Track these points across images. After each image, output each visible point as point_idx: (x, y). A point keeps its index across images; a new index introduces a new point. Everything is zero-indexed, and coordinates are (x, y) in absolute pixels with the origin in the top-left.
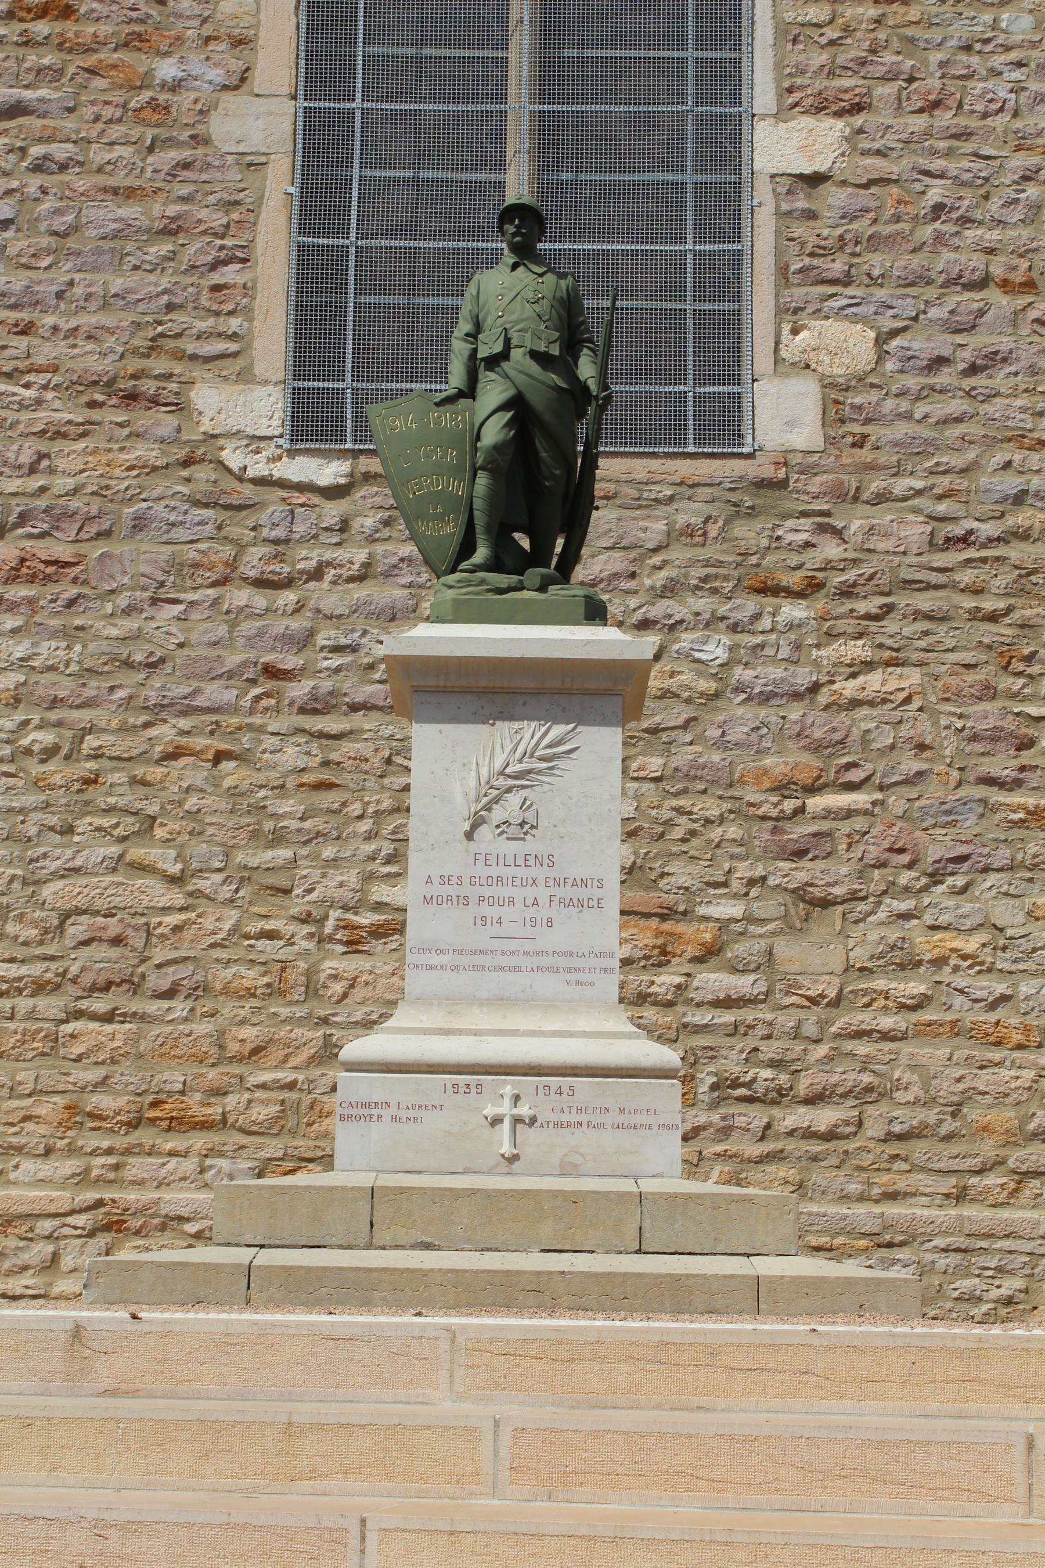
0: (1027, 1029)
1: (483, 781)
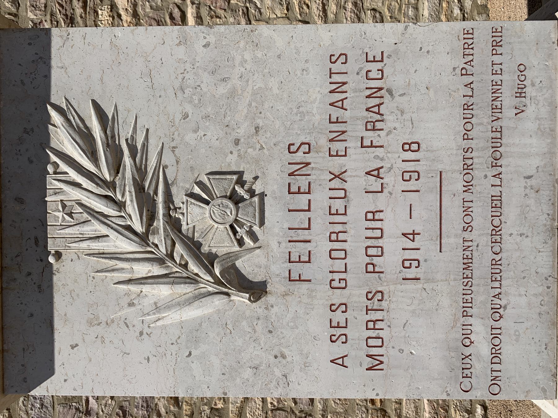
1: (157, 270)
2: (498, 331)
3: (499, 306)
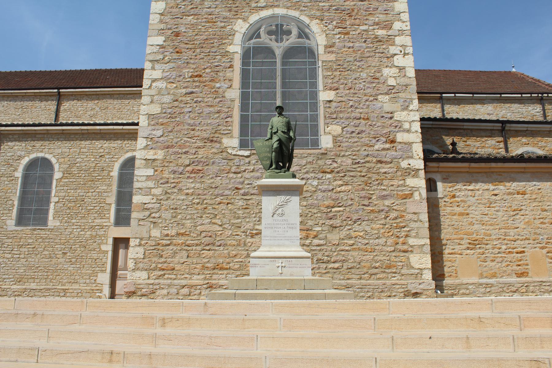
0: (371, 249)
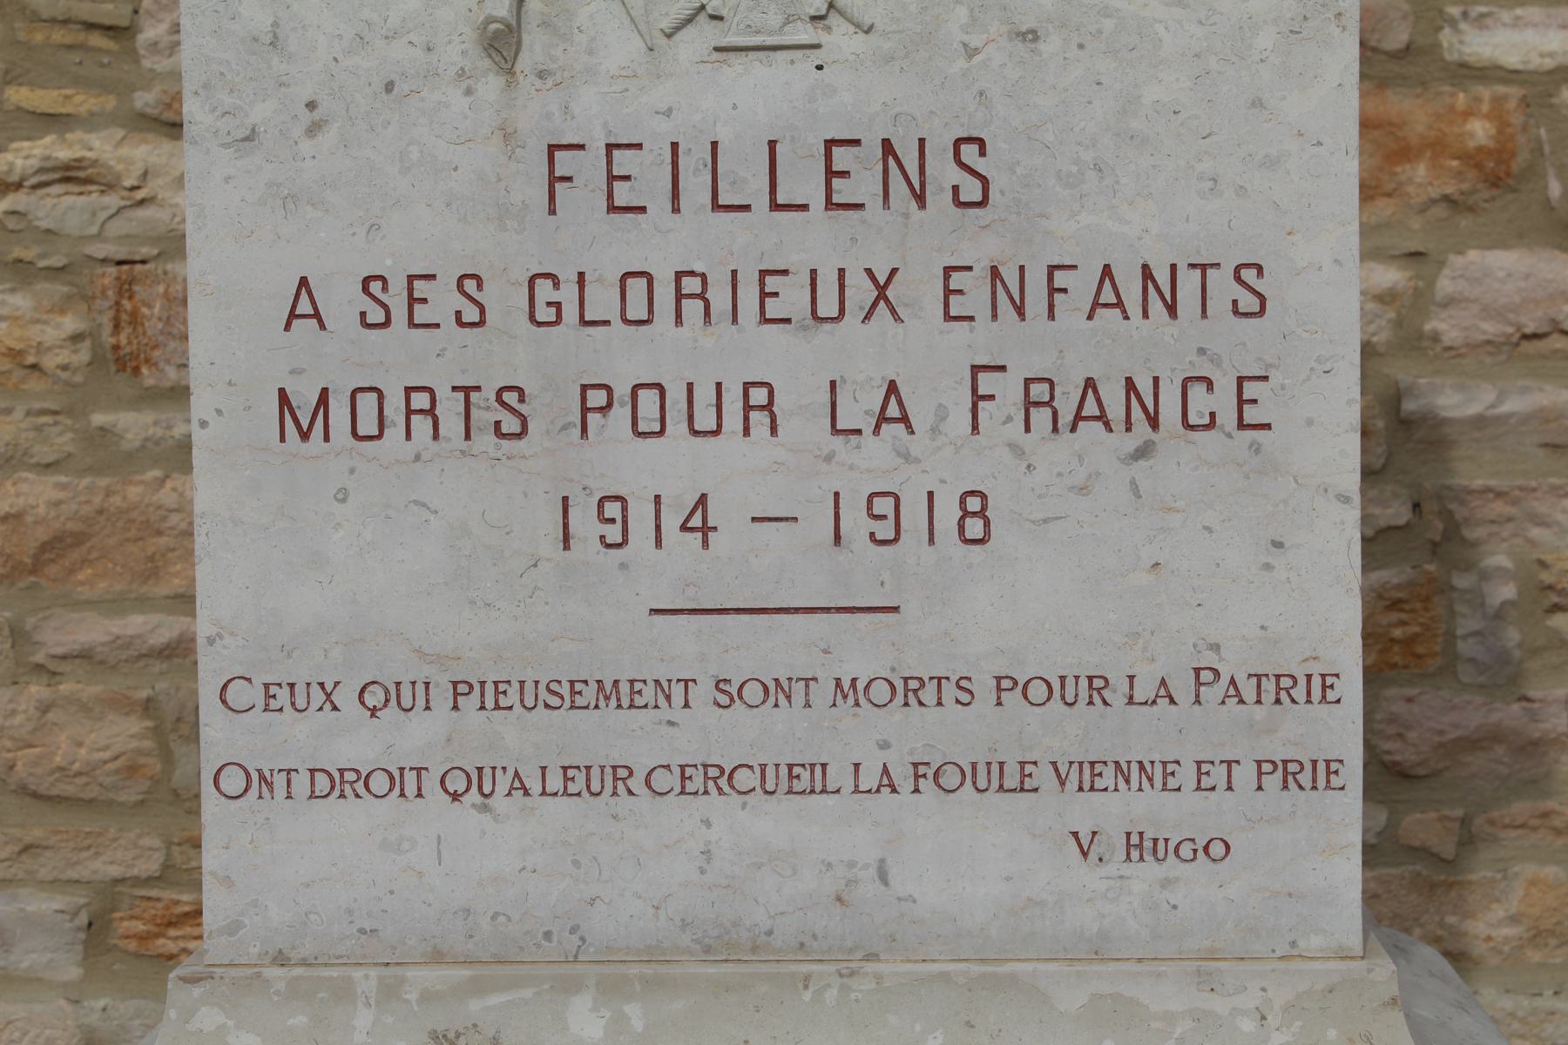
2: (411, 789)
3: (487, 790)
